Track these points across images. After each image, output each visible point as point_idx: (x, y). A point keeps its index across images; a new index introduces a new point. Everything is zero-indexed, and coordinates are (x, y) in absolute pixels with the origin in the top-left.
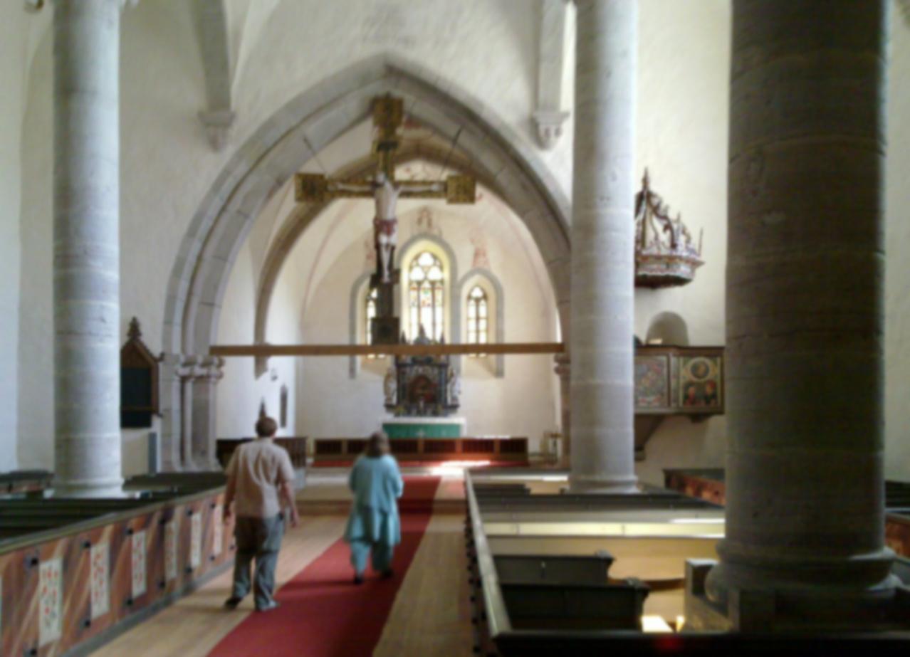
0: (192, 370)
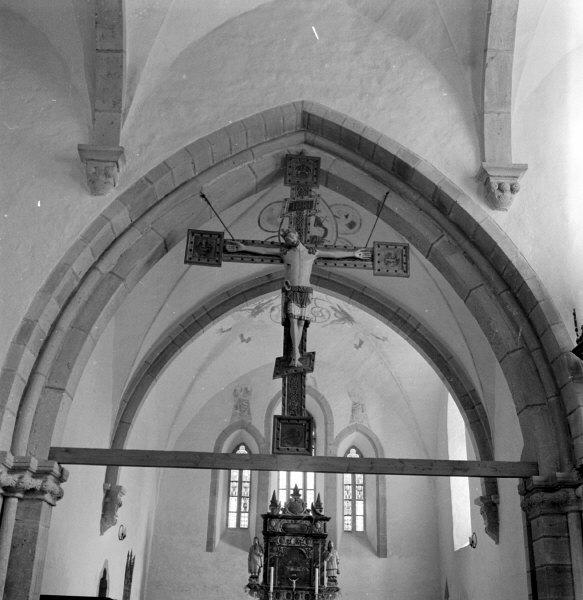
0: (20, 478)
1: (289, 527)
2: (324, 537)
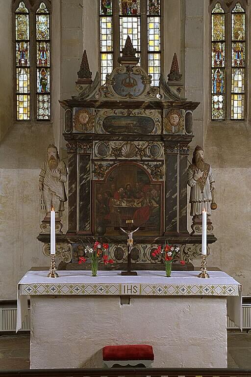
1: (116, 123)
2: (184, 141)
